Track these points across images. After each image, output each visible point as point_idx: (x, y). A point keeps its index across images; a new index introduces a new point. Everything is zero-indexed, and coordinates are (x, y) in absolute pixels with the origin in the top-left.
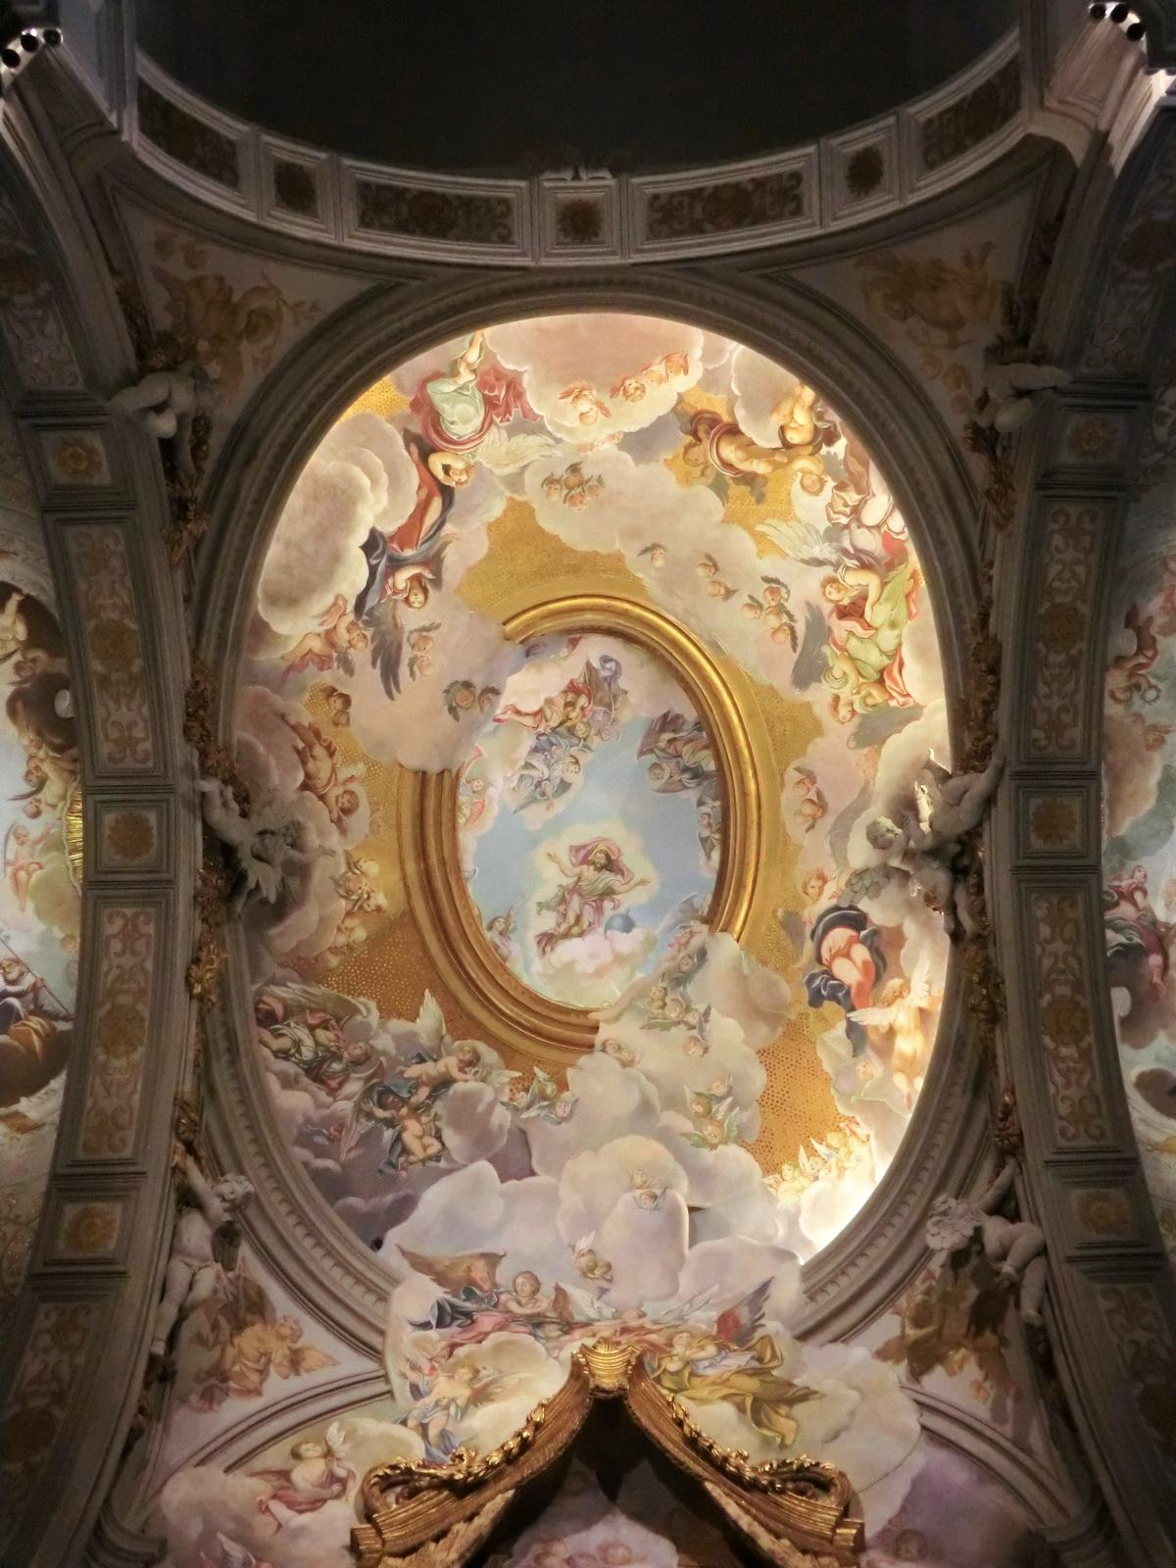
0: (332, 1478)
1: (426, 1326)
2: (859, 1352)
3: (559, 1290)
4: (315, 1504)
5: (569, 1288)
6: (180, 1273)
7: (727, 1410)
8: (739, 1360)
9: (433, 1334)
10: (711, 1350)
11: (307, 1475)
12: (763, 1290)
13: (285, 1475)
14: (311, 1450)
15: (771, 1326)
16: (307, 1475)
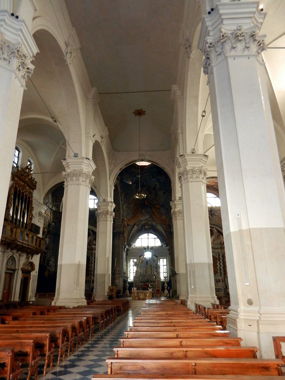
0: (132, 202)
1: (135, 189)
2: (162, 192)
3: (143, 183)
4: (130, 205)
5: (144, 182)
6: (122, 199)
7: (153, 196)
8: (154, 192)
9: (136, 190)
10: (153, 190)
11: (130, 202)
12: (157, 185)
13: (129, 203)
14: (130, 200)
15: (157, 189)
16: (130, 202)
